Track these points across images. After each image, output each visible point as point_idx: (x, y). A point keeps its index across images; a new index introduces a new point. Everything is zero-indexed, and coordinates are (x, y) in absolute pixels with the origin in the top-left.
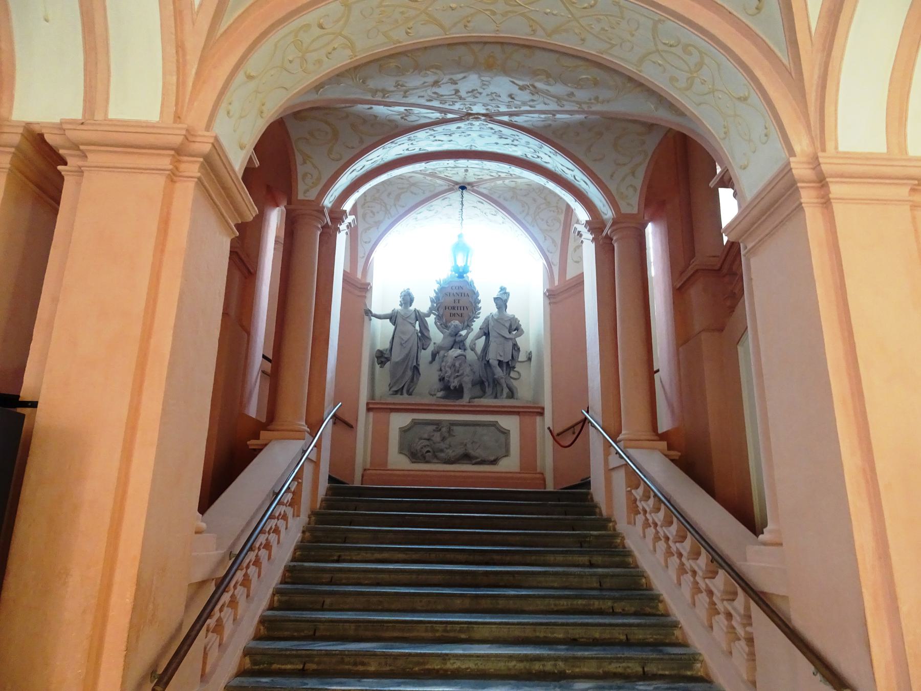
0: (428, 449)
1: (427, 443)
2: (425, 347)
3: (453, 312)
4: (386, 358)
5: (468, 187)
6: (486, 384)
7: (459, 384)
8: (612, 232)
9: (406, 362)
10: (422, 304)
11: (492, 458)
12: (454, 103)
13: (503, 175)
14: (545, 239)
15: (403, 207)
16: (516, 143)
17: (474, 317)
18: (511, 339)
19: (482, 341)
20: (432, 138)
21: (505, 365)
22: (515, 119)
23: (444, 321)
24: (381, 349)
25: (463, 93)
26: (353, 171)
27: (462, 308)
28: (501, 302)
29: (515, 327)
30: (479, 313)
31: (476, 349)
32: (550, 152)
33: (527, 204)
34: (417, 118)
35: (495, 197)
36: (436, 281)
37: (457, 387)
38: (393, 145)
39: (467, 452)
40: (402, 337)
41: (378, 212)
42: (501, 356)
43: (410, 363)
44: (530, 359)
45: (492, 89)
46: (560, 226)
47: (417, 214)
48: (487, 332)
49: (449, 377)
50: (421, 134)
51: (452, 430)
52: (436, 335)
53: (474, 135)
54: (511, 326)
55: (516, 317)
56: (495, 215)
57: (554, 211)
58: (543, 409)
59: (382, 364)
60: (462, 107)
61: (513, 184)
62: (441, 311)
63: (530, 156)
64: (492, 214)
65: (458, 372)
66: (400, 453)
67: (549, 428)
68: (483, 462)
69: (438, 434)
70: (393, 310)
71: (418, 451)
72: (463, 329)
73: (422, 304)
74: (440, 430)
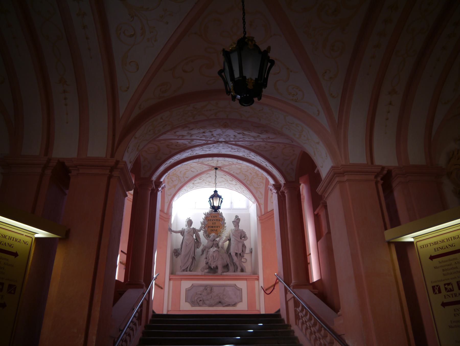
0: (201, 299)
1: (200, 296)
3: (212, 229)
8: (284, 190)
10: (197, 225)
12: (211, 138)
13: (235, 163)
14: (257, 192)
15: (187, 178)
16: (239, 151)
20: (202, 150)
22: (237, 143)
23: (208, 233)
24: (176, 248)
25: (215, 135)
26: (166, 164)
27: (217, 227)
32: (254, 155)
34: (196, 143)
35: (232, 172)
36: (204, 213)
37: (215, 267)
38: (184, 153)
43: (191, 255)
45: (226, 133)
47: (194, 181)
50: (197, 149)
52: (204, 240)
53: (220, 148)
54: (241, 236)
55: (244, 230)
60: (215, 139)
63: (246, 156)
64: (230, 181)
65: (215, 259)
70: (182, 229)
72: (217, 238)
73: (197, 225)
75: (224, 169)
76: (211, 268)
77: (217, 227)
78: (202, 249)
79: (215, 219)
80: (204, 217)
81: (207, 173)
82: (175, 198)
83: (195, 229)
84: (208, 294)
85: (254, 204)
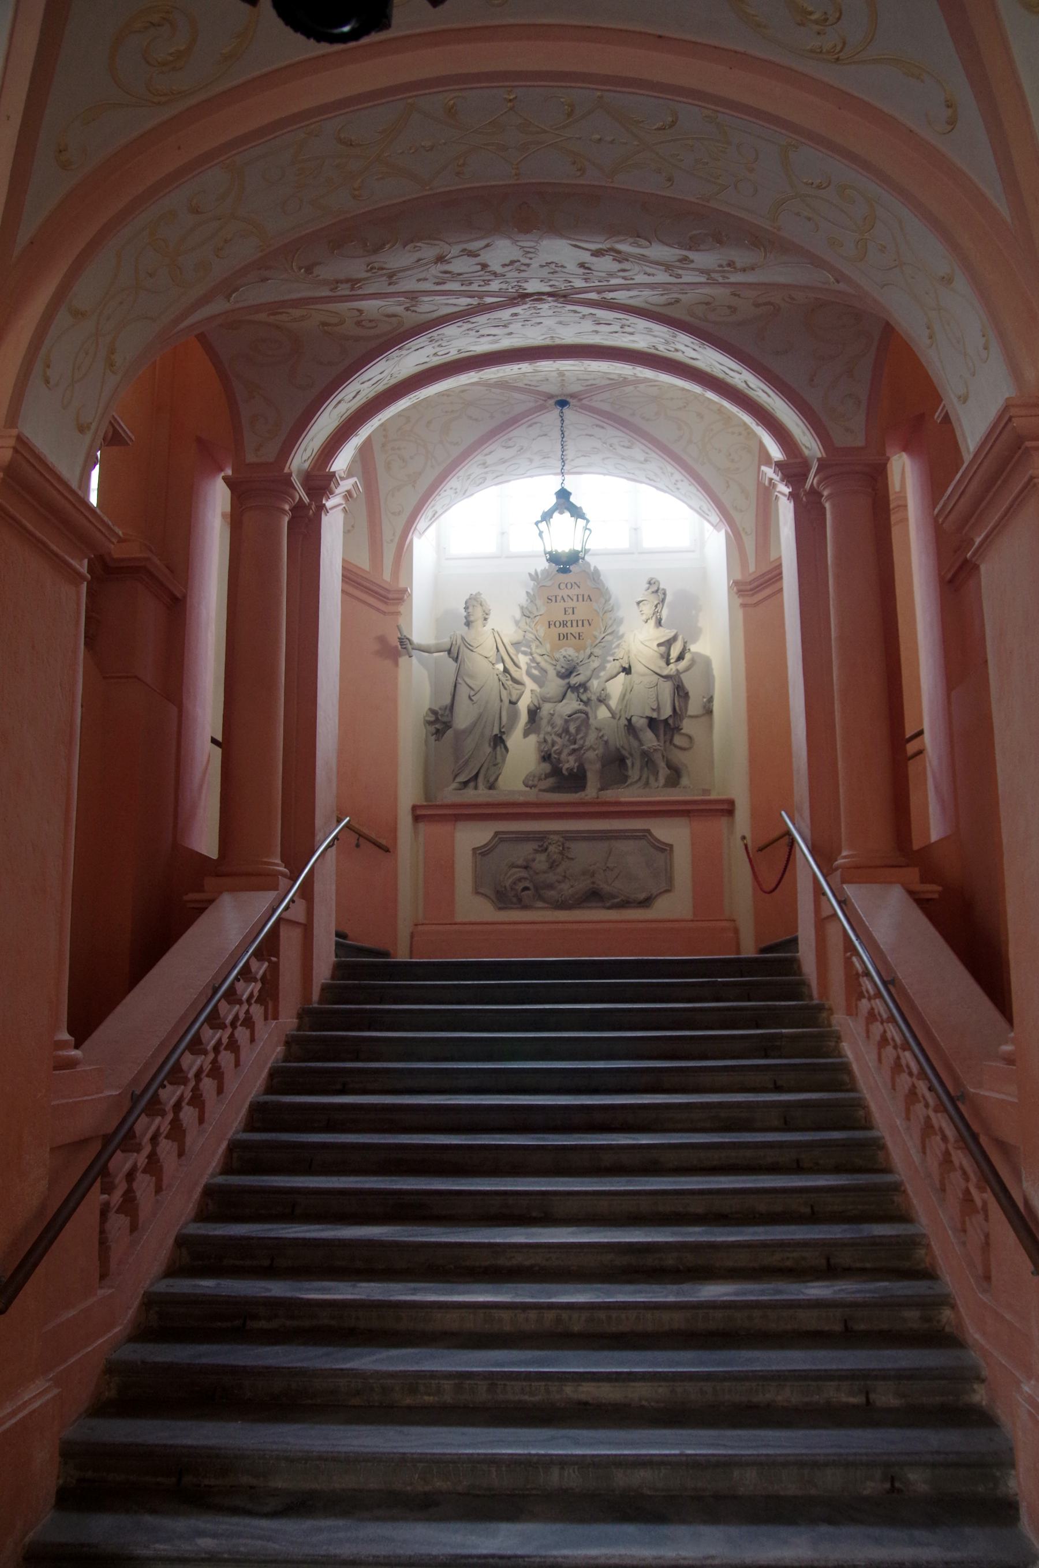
0: (527, 884)
1: (523, 874)
4: (444, 723)
6: (629, 762)
7: (577, 764)
11: (642, 896)
14: (728, 487)
27: (580, 623)
36: (530, 574)
37: (575, 770)
39: (595, 886)
41: (411, 458)
44: (709, 712)
47: (486, 455)
48: (627, 666)
49: (560, 753)
51: (569, 848)
56: (628, 448)
58: (731, 803)
64: (624, 446)
66: (477, 893)
69: (542, 857)
71: (508, 889)
74: (546, 849)
75: (593, 404)
76: (563, 774)
77: (580, 623)
80: (533, 589)
81: (530, 423)
82: (421, 523)
84: (551, 868)
85: (719, 531)
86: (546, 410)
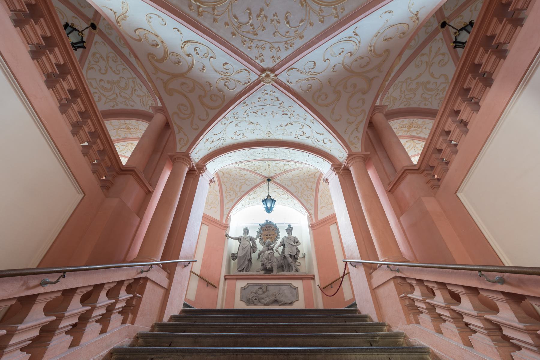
1: (255, 295)
2: (254, 251)
4: (236, 257)
5: (271, 179)
9: (245, 258)
10: (253, 234)
11: (290, 302)
17: (277, 239)
18: (295, 246)
19: (281, 249)
21: (293, 257)
23: (263, 241)
24: (234, 253)
28: (289, 230)
29: (296, 241)
30: (279, 237)
31: (279, 251)
33: (298, 188)
35: (283, 184)
37: (270, 268)
40: (243, 246)
41: (232, 195)
42: (291, 253)
43: (247, 257)
44: (304, 257)
46: (313, 198)
48: (283, 244)
49: (266, 263)
52: (260, 247)
54: (294, 241)
55: (297, 237)
57: (310, 191)
58: (314, 276)
59: (234, 259)
61: (291, 177)
62: (262, 237)
65: (270, 261)
67: (318, 285)
68: (285, 304)
69: (261, 290)
71: (250, 299)
72: (272, 244)
73: (253, 234)
76: (267, 269)
78: (258, 254)
79: (269, 228)
81: (260, 187)
83: (252, 238)
84: (263, 293)
86: (265, 182)
